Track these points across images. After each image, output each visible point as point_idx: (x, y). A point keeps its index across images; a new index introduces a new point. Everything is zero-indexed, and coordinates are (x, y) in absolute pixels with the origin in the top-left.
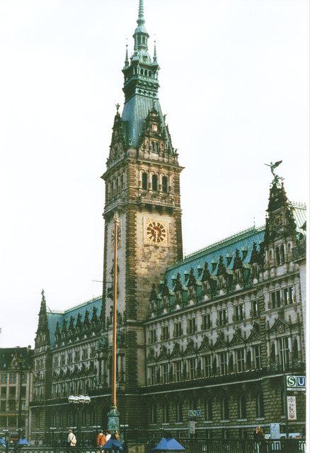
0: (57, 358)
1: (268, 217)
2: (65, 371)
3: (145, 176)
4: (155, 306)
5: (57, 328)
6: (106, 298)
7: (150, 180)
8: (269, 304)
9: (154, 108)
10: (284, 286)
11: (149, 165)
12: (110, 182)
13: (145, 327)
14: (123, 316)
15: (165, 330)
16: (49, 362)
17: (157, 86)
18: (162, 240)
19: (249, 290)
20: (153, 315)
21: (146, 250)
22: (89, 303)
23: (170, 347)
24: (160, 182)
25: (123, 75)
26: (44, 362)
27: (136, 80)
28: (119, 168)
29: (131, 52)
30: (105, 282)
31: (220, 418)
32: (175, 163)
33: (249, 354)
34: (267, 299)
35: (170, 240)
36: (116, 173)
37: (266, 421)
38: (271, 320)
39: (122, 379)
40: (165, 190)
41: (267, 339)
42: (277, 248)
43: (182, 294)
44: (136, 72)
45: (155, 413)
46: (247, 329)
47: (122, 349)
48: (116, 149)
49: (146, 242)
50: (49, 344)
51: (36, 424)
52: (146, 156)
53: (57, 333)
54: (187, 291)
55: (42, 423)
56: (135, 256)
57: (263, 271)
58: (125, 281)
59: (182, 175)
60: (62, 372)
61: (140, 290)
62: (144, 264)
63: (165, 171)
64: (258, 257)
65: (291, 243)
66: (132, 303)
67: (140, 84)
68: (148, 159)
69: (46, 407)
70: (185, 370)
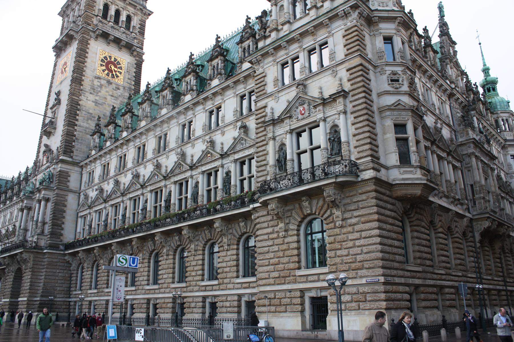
13: (82, 167)
18: (117, 77)
21: (96, 83)
23: (108, 187)
33: (228, 173)
35: (126, 79)
37: (261, 282)
41: (270, 135)
43: (132, 117)
47: (47, 192)
49: (99, 73)
56: (82, 85)
61: (82, 124)
62: (92, 97)
63: (130, 8)
70: (124, 216)
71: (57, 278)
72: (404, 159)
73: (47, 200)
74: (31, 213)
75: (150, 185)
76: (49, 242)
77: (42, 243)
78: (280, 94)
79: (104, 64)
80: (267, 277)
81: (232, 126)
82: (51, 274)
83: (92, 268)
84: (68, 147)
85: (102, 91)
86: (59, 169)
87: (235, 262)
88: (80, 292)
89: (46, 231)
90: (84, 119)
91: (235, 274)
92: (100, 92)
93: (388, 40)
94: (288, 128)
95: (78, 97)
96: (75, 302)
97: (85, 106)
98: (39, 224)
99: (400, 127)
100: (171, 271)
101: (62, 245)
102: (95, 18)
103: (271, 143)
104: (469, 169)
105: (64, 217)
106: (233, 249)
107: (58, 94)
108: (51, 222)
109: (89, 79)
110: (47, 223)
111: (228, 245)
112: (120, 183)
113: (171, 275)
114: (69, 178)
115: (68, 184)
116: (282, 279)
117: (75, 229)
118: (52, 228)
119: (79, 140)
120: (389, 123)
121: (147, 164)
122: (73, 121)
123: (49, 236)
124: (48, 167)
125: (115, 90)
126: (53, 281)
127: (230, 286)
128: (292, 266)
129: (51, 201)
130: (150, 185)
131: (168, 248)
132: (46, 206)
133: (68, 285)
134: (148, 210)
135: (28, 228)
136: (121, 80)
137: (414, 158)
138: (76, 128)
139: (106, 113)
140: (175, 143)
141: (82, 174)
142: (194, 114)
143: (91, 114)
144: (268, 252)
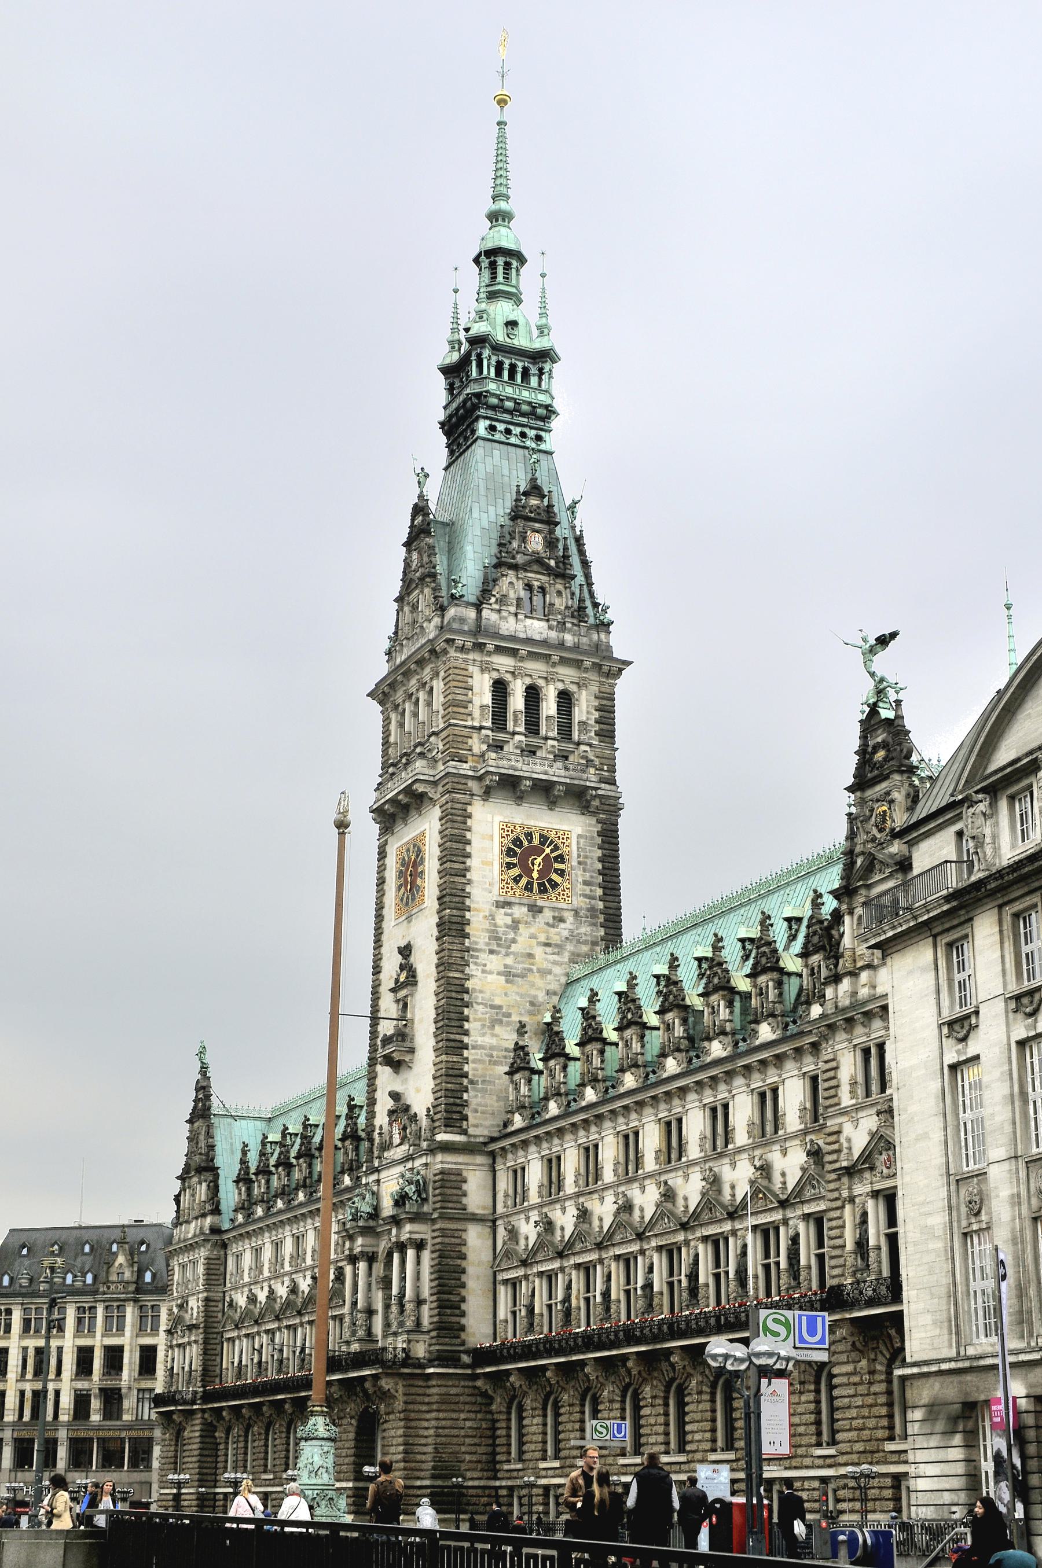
1: (853, 810)
2: (262, 1296)
3: (500, 689)
4: (524, 1090)
5: (243, 1162)
6: (379, 1068)
7: (517, 702)
8: (854, 1084)
9: (534, 480)
11: (513, 653)
12: (396, 707)
14: (424, 1122)
15: (553, 1164)
16: (215, 1273)
17: (550, 411)
19: (802, 1041)
20: (518, 1121)
21: (502, 918)
23: (566, 1220)
24: (549, 707)
25: (441, 381)
26: (201, 1269)
27: (478, 395)
28: (421, 663)
30: (375, 1019)
31: (708, 1446)
32: (602, 651)
33: (795, 1240)
37: (842, 1459)
38: (857, 1135)
39: (418, 1323)
40: (565, 731)
41: (845, 1194)
44: (481, 372)
45: (521, 1427)
46: (790, 1164)
48: (414, 608)
51: (175, 1463)
52: (509, 626)
53: (243, 1179)
54: (616, 1044)
55: (192, 1460)
56: (467, 936)
58: (432, 1014)
60: (252, 1299)
61: (480, 1040)
62: (495, 963)
64: (823, 938)
66: (453, 1085)
67: (493, 408)
68: (513, 638)
69: (203, 1411)
70: (606, 1294)
71: (462, 1432)
73: (420, 1246)
74: (379, 1268)
75: (656, 1235)
76: (437, 1347)
77: (420, 1351)
78: (860, 1115)
79: (515, 860)
80: (849, 1450)
81: (797, 1142)
82: (449, 1423)
83: (544, 1409)
84: (454, 1108)
85: (518, 938)
86: (439, 1166)
87: (813, 1416)
88: (519, 1466)
89: (426, 1322)
90: (483, 1026)
91: (813, 1440)
92: (514, 941)
94: (868, 1188)
95: (463, 972)
96: (511, 1489)
97: (481, 992)
98: (409, 1307)
100: (707, 1425)
101: (467, 1352)
102: (475, 736)
103: (848, 1207)
105: (463, 1286)
106: (809, 1391)
107: (406, 951)
108: (434, 1298)
109: (481, 914)
110: (424, 1301)
111: (802, 1383)
112: (591, 1214)
113: (708, 1435)
114: (465, 1187)
115: (464, 1200)
117: (491, 1310)
118: (439, 1314)
119: (477, 1083)
121: (647, 1182)
122: (458, 1037)
123: (433, 1334)
124: (410, 1158)
125: (553, 926)
126: (455, 1440)
127: (807, 1461)
128: (880, 1434)
129: (429, 1247)
130: (656, 1235)
131: (700, 1379)
132: (418, 1262)
133: (490, 1449)
134: (655, 1290)
135: (374, 1307)
138: (466, 1053)
139: (535, 997)
140: (698, 1149)
141: (494, 1172)
142: (730, 1092)
143: (500, 1007)
144: (849, 1407)
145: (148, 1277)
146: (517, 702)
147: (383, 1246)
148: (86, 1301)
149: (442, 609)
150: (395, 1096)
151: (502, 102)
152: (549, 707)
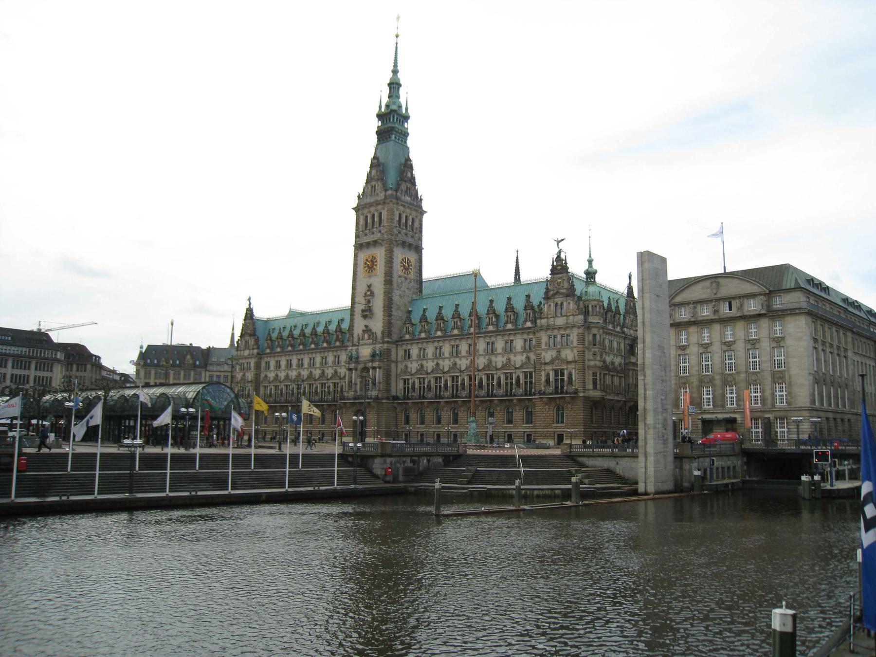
0: (268, 363)
3: (400, 214)
7: (403, 220)
10: (562, 332)
11: (404, 206)
12: (363, 214)
16: (258, 366)
22: (302, 314)
24: (410, 223)
26: (252, 365)
27: (393, 128)
29: (385, 100)
32: (421, 207)
34: (544, 339)
36: (372, 209)
42: (556, 304)
50: (258, 348)
57: (541, 318)
58: (382, 305)
59: (426, 219)
63: (414, 213)
65: (571, 302)
67: (397, 132)
72: (595, 388)
77: (380, 396)
93: (594, 336)
99: (594, 374)
104: (629, 376)
116: (544, 427)
120: (591, 373)
136: (412, 275)
137: (598, 386)
145: (198, 363)
146: (403, 220)
147: (361, 366)
148: (178, 369)
149: (386, 190)
150: (366, 326)
151: (397, 36)
152: (410, 223)
